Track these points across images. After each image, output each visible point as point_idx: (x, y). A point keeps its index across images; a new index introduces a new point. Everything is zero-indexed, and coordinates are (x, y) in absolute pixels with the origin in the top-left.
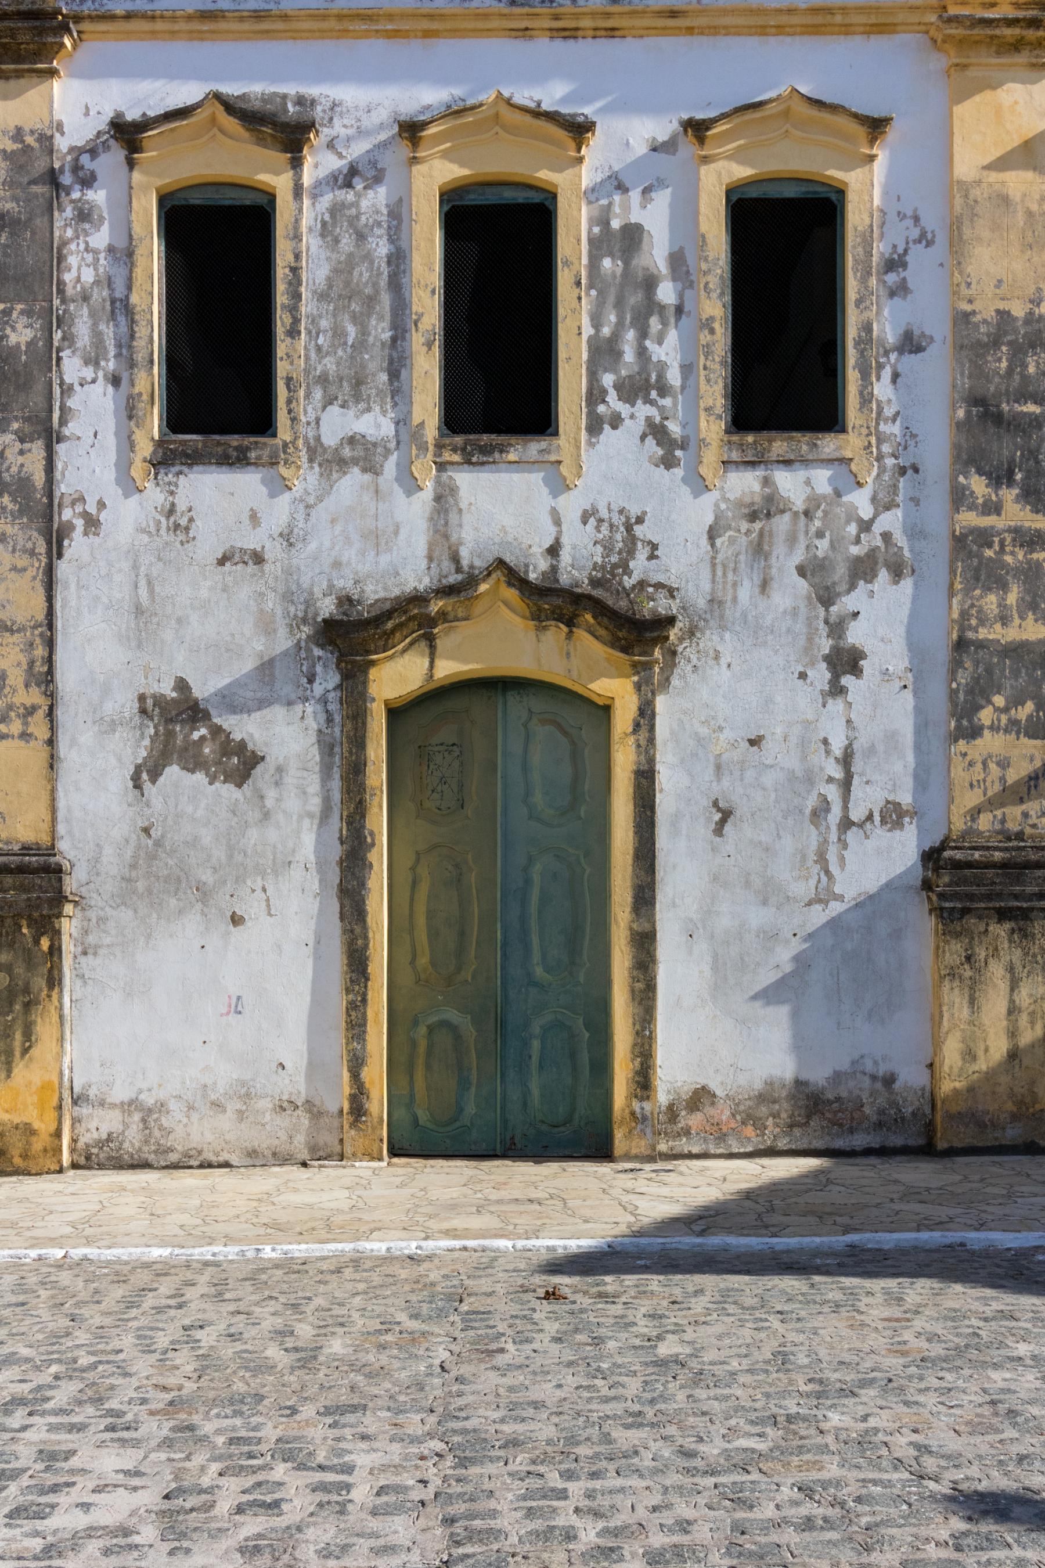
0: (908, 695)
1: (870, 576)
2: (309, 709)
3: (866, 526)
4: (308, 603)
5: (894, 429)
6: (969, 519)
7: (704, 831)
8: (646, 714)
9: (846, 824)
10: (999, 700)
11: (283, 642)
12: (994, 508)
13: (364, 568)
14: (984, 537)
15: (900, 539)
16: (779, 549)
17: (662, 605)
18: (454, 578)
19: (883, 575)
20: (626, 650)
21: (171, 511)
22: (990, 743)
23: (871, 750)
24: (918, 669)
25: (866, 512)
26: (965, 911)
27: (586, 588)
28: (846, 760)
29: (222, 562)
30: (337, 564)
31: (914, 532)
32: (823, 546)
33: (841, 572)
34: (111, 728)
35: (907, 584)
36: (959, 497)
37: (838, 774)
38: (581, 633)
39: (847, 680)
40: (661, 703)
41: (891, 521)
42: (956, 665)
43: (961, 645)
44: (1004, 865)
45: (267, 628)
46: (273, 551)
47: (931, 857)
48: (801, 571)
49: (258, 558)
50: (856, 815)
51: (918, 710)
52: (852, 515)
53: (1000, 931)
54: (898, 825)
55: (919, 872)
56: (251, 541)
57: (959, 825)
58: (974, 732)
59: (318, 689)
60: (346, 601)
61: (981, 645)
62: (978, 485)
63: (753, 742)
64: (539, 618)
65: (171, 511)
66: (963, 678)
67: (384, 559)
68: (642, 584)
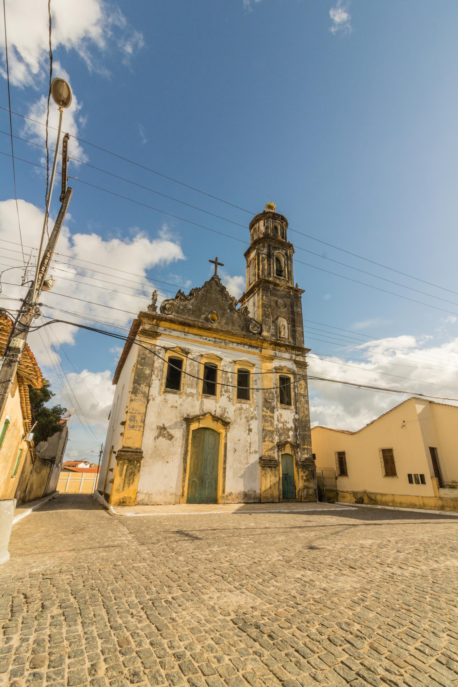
0: (257, 436)
1: (253, 419)
2: (182, 430)
3: (252, 413)
4: (183, 414)
5: (256, 401)
6: (264, 413)
7: (233, 452)
8: (226, 435)
9: (250, 453)
10: (268, 437)
11: (179, 420)
12: (267, 412)
13: (191, 411)
14: (266, 416)
15: (256, 415)
16: (242, 414)
17: (228, 420)
18: (203, 413)
19: (254, 419)
20: (224, 426)
21: (165, 399)
22: (267, 443)
23: (253, 443)
24: (258, 432)
25: (252, 411)
26: (265, 466)
27: (219, 417)
28: (250, 444)
29: (171, 407)
30: (187, 410)
31: (258, 414)
32: (248, 414)
33: (250, 418)
34: (152, 430)
35: (257, 421)
36: (263, 411)
37: (249, 446)
38: (219, 423)
39: (250, 433)
40: (228, 434)
41: (255, 412)
42: (263, 432)
43: (263, 429)
44: (269, 460)
45: (177, 418)
46: (179, 407)
47: (260, 458)
48: (245, 418)
49: (176, 407)
50: (251, 452)
51: (259, 438)
52: (251, 411)
53: (269, 469)
54: (256, 453)
55: (259, 461)
56: (176, 405)
57: (263, 454)
58: (265, 441)
59: (183, 427)
60: (188, 415)
61: (266, 430)
62: (265, 409)
63: (239, 440)
64: (213, 420)
65: (165, 399)
66: (264, 434)
67: (194, 410)
68: (226, 417)
